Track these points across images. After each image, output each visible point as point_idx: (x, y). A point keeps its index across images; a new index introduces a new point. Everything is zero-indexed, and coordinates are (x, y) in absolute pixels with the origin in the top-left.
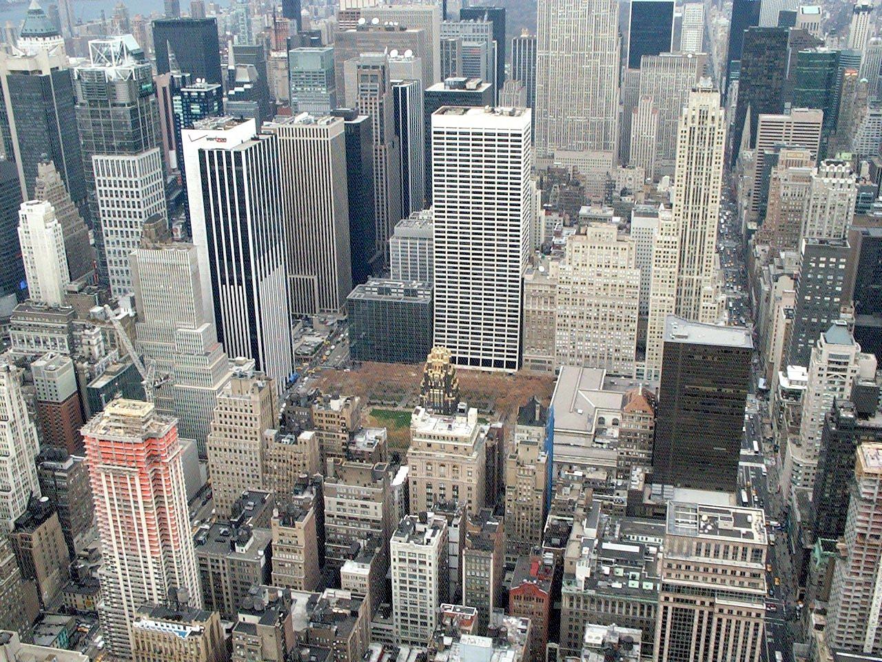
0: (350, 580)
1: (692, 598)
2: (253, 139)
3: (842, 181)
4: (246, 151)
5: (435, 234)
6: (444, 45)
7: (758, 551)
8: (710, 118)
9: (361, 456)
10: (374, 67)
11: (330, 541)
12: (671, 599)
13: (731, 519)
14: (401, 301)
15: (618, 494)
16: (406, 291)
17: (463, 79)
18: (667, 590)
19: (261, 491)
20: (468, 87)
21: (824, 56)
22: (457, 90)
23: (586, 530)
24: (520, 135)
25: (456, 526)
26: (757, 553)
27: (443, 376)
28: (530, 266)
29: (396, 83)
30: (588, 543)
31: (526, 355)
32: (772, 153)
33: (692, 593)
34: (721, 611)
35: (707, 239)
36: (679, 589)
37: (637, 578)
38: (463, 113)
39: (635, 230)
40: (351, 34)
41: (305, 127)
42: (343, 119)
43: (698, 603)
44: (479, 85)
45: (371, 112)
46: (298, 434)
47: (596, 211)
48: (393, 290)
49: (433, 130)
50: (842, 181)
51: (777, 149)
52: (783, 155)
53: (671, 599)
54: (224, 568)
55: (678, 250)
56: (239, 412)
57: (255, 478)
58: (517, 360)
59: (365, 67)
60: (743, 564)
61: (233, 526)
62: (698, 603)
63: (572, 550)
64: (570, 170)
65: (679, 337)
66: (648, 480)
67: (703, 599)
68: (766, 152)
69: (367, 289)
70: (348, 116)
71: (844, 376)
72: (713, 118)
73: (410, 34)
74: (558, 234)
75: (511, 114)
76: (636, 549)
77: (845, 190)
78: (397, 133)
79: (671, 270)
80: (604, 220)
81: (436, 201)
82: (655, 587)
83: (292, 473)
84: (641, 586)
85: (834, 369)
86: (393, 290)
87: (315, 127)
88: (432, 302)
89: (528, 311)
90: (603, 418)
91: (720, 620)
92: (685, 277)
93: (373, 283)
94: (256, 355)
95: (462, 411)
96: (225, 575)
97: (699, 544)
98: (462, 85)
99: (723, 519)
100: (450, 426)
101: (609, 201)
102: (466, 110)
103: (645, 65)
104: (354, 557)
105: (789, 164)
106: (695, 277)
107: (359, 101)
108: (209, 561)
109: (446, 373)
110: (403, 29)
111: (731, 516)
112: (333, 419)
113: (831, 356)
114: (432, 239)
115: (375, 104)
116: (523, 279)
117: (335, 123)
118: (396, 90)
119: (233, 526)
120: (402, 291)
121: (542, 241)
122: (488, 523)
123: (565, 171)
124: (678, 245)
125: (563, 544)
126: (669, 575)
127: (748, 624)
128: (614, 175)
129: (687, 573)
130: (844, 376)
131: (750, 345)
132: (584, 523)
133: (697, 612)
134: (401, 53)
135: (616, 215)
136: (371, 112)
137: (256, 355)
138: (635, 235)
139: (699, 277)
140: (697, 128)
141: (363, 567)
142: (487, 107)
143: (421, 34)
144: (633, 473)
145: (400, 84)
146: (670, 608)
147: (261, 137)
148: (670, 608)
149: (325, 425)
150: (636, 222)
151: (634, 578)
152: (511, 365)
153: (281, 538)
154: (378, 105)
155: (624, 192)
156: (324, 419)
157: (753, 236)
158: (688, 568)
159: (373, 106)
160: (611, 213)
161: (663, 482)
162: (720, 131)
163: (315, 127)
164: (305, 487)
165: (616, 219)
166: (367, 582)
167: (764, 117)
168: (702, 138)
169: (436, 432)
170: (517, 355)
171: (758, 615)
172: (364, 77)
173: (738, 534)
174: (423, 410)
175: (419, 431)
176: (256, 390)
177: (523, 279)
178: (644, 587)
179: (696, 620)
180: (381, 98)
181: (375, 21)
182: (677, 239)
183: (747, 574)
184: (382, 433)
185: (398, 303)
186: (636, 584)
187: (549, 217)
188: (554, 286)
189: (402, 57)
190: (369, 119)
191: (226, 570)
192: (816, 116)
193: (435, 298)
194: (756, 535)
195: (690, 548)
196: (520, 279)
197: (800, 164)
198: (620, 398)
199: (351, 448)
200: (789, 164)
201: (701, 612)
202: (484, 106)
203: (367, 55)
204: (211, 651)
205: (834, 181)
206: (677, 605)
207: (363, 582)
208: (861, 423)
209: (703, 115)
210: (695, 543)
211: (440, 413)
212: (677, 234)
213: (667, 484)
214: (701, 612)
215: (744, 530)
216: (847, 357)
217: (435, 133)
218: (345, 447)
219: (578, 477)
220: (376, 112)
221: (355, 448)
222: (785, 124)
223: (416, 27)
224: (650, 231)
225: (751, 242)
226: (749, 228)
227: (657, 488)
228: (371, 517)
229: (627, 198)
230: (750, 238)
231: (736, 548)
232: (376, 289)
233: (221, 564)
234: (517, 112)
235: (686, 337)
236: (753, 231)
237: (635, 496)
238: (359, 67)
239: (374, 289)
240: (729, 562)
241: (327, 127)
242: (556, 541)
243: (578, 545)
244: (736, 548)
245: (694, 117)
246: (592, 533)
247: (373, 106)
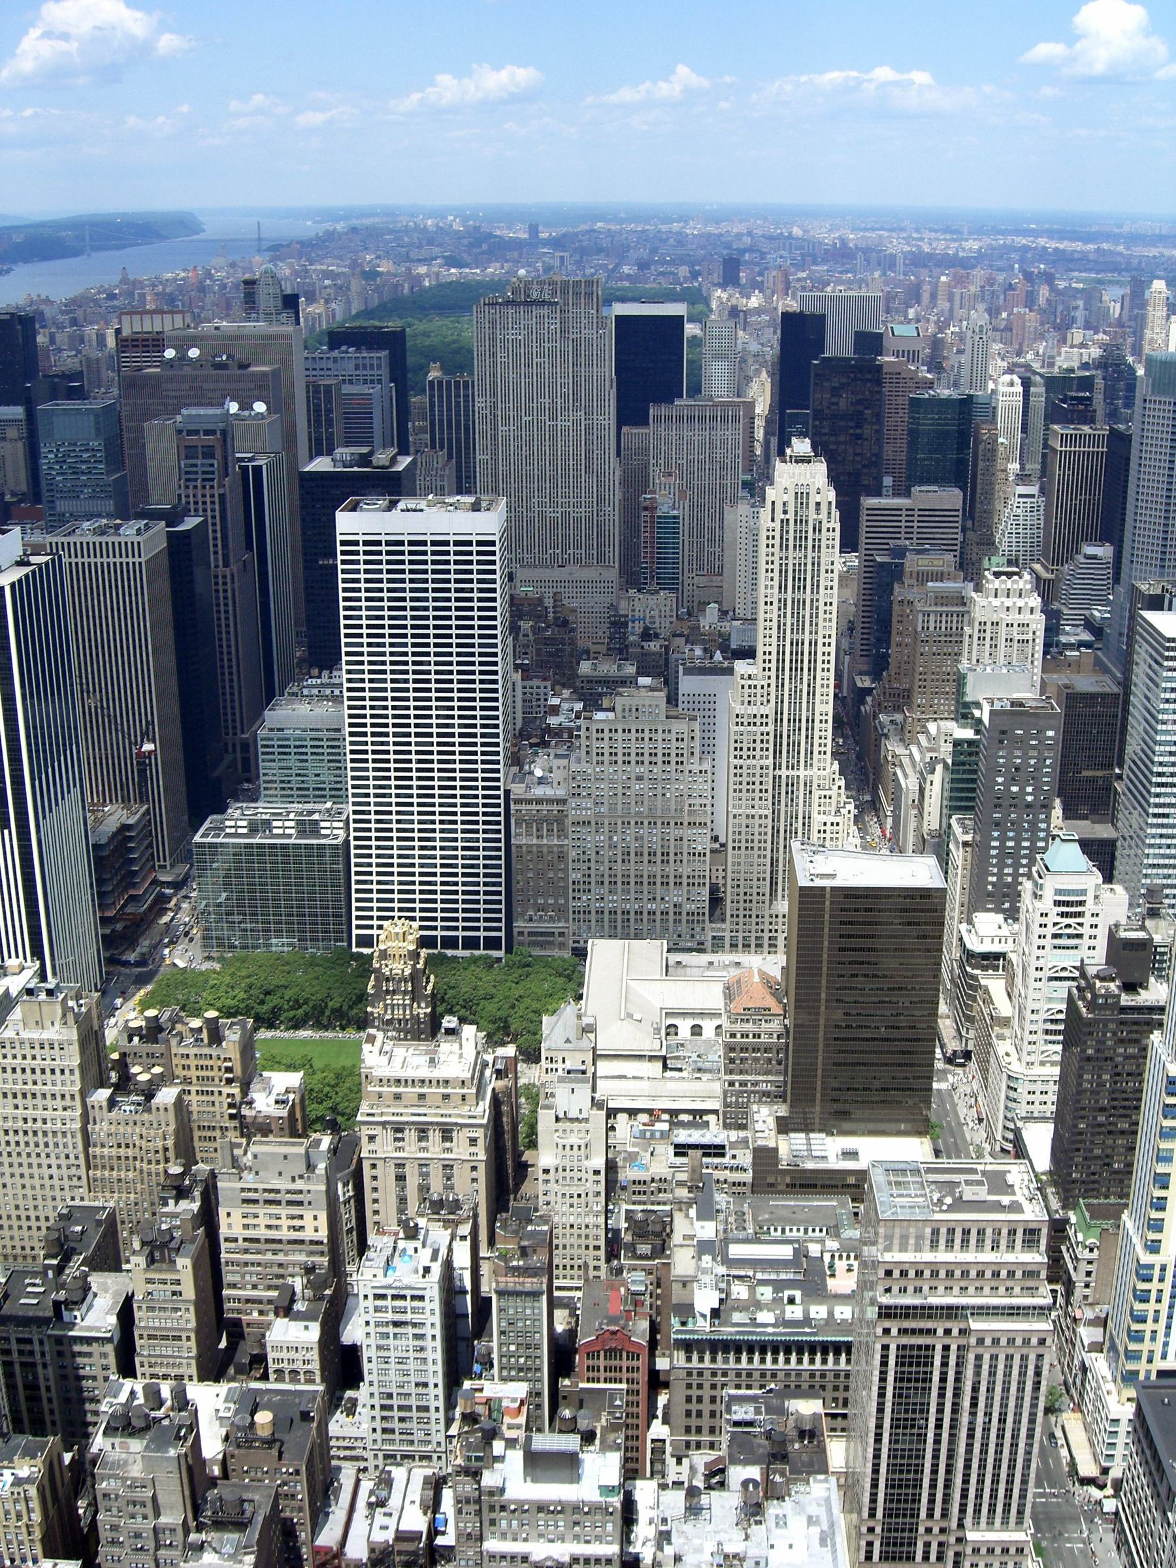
0: (284, 1355)
1: (929, 1325)
2: (21, 563)
3: (1020, 603)
4: (13, 585)
5: (348, 721)
6: (313, 390)
7: (1032, 1232)
8: (812, 506)
9: (263, 1128)
10: (207, 433)
11: (233, 1286)
12: (894, 1332)
13: (980, 1183)
14: (292, 841)
15: (734, 1157)
16: (298, 822)
17: (365, 450)
18: (888, 1316)
19: (86, 1203)
20: (375, 463)
21: (948, 401)
22: (356, 469)
23: (698, 1224)
24: (493, 543)
25: (463, 1238)
26: (1031, 1236)
27: (408, 972)
28: (515, 769)
29: (242, 459)
30: (704, 1247)
31: (519, 924)
33: (930, 1317)
34: (981, 1341)
35: (819, 708)
36: (906, 1312)
37: (798, 1300)
38: (389, 509)
39: (686, 699)
40: (155, 375)
41: (98, 539)
42: (163, 523)
43: (940, 1332)
44: (393, 461)
45: (205, 510)
46: (150, 1096)
47: (608, 668)
48: (275, 824)
49: (339, 538)
50: (1020, 603)
51: (900, 553)
52: (913, 563)
53: (894, 1332)
54: (43, 1354)
55: (770, 728)
56: (19, 1060)
57: (75, 1182)
58: (502, 934)
59: (190, 433)
60: (1010, 1257)
61: (50, 1274)
62: (940, 1332)
63: (682, 1262)
64: (549, 602)
65: (823, 876)
66: (784, 1126)
67: (948, 1325)
68: (879, 559)
69: (228, 823)
70: (172, 518)
71: (1081, 925)
72: (818, 504)
73: (255, 374)
74: (555, 710)
75: (476, 507)
76: (785, 1252)
77: (1026, 617)
78: (249, 547)
79: (762, 762)
80: (624, 682)
82: (831, 1314)
83: (145, 1165)
84: (831, 1314)
85: (1063, 915)
86: (275, 824)
87: (116, 539)
88: (347, 842)
89: (519, 846)
90: (676, 1027)
91: (979, 1358)
92: (784, 773)
93: (234, 811)
94: (37, 952)
95: (451, 1032)
96: (45, 1366)
97: (936, 1232)
98: (365, 460)
99: (967, 1183)
100: (432, 1061)
101: (621, 651)
102: (392, 505)
103: (658, 419)
104: (286, 1309)
105: (923, 578)
106: (802, 773)
107: (182, 492)
108: (14, 1342)
109: (414, 966)
110: (244, 366)
111: (978, 1177)
112: (209, 1063)
113: (1059, 892)
115: (212, 496)
116: (507, 793)
117: (151, 532)
118: (244, 470)
119: (50, 1274)
120: (292, 824)
121: (519, 725)
122: (529, 1228)
123: (540, 600)
124: (771, 720)
125: (661, 1248)
126: (888, 1290)
127: (1010, 1358)
128: (623, 608)
129: (918, 1283)
130: (1081, 925)
131: (937, 882)
132: (693, 1212)
133: (939, 1348)
134: (246, 406)
135: (640, 673)
136: (205, 510)
137: (37, 952)
138: (686, 705)
139: (808, 773)
140: (792, 522)
141: (306, 1328)
142: (430, 497)
143: (276, 374)
144: (756, 1117)
145: (250, 460)
146: (893, 1347)
147: (34, 559)
148: (893, 1347)
149: (193, 1073)
150: (688, 685)
151: (791, 1301)
152: (492, 943)
153: (150, 1287)
154: (217, 499)
155: (647, 635)
156: (193, 1062)
157: (869, 699)
158: (919, 1274)
159: (208, 499)
160: (631, 670)
161: (807, 1128)
162: (831, 526)
163: (116, 539)
164: (182, 1193)
165: (644, 681)
166: (315, 1355)
168: (801, 538)
169: (410, 1073)
170: (503, 925)
171: (1042, 1342)
172: (190, 452)
173: (998, 1207)
174: (380, 1036)
175: (377, 1073)
176: (70, 1018)
177: (507, 793)
178: (838, 1316)
179: (937, 1362)
180: (222, 486)
181: (194, 353)
182: (769, 710)
183: (1019, 1274)
184: (294, 1079)
185: (284, 847)
186: (794, 1312)
187: (528, 683)
188: (564, 802)
189: (246, 413)
190: (204, 523)
191: (48, 1357)
192: (951, 498)
193: (353, 834)
194: (1026, 1205)
195: (919, 1237)
196: (501, 793)
197: (939, 577)
198: (718, 989)
199: (245, 1111)
200: (923, 578)
201: (946, 1348)
202: (427, 495)
203: (193, 411)
204: (52, 1512)
205: (1008, 602)
206: (905, 1341)
207: (308, 1357)
208: (1126, 1000)
209: (801, 498)
210: (928, 1231)
211: (405, 1039)
213: (813, 1131)
214: (946, 1348)
215: (1006, 1200)
216: (1083, 892)
217: (343, 543)
218: (234, 1111)
219: (662, 1132)
220: (213, 510)
221: (253, 1113)
222: (904, 513)
223: (263, 364)
224: (712, 699)
225: (866, 709)
226: (859, 685)
227: (798, 1139)
228: (308, 1234)
229: (652, 644)
230: (863, 702)
231: (951, 1232)
232: (244, 823)
233: (37, 1347)
234: (484, 504)
235: (833, 876)
236: (869, 691)
237: (765, 1157)
238: (180, 432)
239: (240, 823)
240: (988, 1256)
241: (139, 539)
242: (644, 1248)
243: (691, 1252)
244: (951, 1232)
246: (707, 1230)
247: (208, 499)
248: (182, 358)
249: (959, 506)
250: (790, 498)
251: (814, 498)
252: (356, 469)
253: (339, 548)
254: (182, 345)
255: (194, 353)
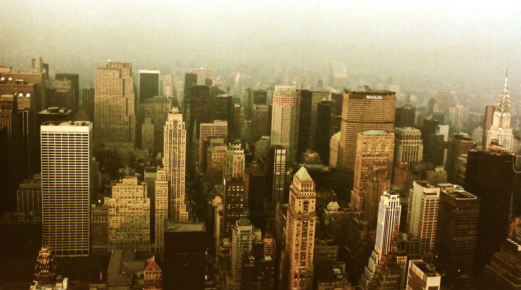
3: (238, 152)
17: (57, 108)
21: (225, 98)
22: (54, 113)
24: (87, 135)
29: (21, 110)
32: (207, 140)
35: (181, 181)
49: (41, 133)
52: (212, 141)
68: (205, 140)
77: (240, 156)
81: (43, 169)
98: (57, 111)
105: (215, 145)
114: (41, 189)
116: (90, 207)
128: (135, 153)
135: (136, 172)
142: (70, 122)
150: (147, 175)
157: (202, 179)
160: (134, 171)
162: (184, 131)
165: (136, 174)
167: (202, 125)
181: (10, 79)
182: (166, 182)
197: (219, 145)
200: (215, 145)
212: (167, 179)
217: (42, 134)
236: (202, 176)
245: (171, 126)
248: (6, 81)
249: (227, 126)
250: (172, 123)
251: (179, 123)
252: (54, 113)
253: (41, 136)
254: (7, 76)
255: (10, 79)
